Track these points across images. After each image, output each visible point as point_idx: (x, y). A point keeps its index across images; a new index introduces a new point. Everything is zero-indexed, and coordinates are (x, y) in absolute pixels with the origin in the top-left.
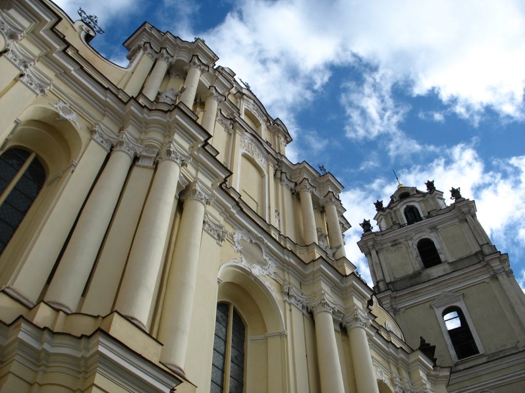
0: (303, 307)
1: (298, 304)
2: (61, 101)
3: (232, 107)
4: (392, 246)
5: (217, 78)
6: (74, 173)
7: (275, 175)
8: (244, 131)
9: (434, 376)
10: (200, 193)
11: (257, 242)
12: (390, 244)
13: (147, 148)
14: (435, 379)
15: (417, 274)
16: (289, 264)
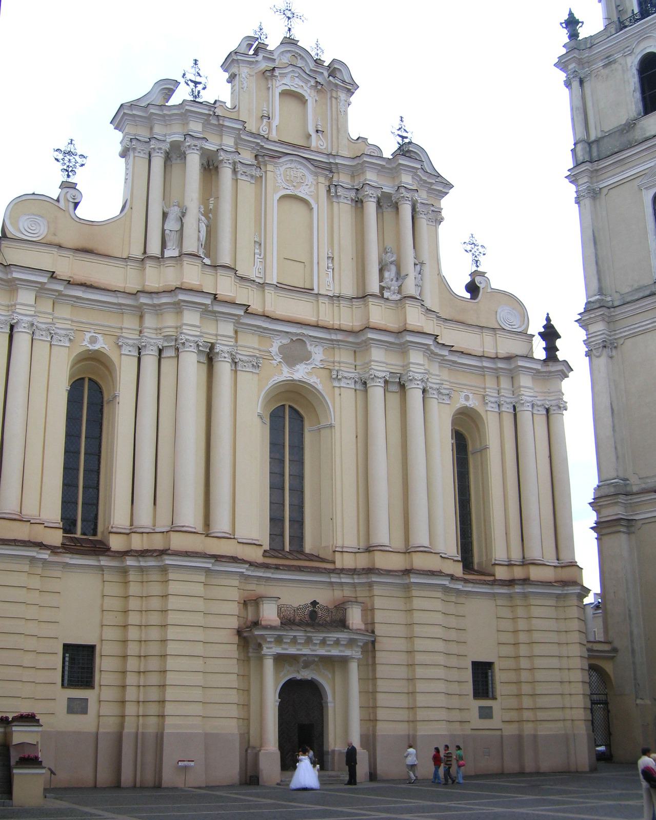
0: (355, 382)
1: (348, 384)
3: (255, 138)
4: (605, 66)
5: (223, 125)
6: (120, 403)
7: (329, 191)
8: (276, 160)
10: (222, 351)
11: (298, 338)
12: (601, 64)
13: (166, 338)
15: (630, 126)
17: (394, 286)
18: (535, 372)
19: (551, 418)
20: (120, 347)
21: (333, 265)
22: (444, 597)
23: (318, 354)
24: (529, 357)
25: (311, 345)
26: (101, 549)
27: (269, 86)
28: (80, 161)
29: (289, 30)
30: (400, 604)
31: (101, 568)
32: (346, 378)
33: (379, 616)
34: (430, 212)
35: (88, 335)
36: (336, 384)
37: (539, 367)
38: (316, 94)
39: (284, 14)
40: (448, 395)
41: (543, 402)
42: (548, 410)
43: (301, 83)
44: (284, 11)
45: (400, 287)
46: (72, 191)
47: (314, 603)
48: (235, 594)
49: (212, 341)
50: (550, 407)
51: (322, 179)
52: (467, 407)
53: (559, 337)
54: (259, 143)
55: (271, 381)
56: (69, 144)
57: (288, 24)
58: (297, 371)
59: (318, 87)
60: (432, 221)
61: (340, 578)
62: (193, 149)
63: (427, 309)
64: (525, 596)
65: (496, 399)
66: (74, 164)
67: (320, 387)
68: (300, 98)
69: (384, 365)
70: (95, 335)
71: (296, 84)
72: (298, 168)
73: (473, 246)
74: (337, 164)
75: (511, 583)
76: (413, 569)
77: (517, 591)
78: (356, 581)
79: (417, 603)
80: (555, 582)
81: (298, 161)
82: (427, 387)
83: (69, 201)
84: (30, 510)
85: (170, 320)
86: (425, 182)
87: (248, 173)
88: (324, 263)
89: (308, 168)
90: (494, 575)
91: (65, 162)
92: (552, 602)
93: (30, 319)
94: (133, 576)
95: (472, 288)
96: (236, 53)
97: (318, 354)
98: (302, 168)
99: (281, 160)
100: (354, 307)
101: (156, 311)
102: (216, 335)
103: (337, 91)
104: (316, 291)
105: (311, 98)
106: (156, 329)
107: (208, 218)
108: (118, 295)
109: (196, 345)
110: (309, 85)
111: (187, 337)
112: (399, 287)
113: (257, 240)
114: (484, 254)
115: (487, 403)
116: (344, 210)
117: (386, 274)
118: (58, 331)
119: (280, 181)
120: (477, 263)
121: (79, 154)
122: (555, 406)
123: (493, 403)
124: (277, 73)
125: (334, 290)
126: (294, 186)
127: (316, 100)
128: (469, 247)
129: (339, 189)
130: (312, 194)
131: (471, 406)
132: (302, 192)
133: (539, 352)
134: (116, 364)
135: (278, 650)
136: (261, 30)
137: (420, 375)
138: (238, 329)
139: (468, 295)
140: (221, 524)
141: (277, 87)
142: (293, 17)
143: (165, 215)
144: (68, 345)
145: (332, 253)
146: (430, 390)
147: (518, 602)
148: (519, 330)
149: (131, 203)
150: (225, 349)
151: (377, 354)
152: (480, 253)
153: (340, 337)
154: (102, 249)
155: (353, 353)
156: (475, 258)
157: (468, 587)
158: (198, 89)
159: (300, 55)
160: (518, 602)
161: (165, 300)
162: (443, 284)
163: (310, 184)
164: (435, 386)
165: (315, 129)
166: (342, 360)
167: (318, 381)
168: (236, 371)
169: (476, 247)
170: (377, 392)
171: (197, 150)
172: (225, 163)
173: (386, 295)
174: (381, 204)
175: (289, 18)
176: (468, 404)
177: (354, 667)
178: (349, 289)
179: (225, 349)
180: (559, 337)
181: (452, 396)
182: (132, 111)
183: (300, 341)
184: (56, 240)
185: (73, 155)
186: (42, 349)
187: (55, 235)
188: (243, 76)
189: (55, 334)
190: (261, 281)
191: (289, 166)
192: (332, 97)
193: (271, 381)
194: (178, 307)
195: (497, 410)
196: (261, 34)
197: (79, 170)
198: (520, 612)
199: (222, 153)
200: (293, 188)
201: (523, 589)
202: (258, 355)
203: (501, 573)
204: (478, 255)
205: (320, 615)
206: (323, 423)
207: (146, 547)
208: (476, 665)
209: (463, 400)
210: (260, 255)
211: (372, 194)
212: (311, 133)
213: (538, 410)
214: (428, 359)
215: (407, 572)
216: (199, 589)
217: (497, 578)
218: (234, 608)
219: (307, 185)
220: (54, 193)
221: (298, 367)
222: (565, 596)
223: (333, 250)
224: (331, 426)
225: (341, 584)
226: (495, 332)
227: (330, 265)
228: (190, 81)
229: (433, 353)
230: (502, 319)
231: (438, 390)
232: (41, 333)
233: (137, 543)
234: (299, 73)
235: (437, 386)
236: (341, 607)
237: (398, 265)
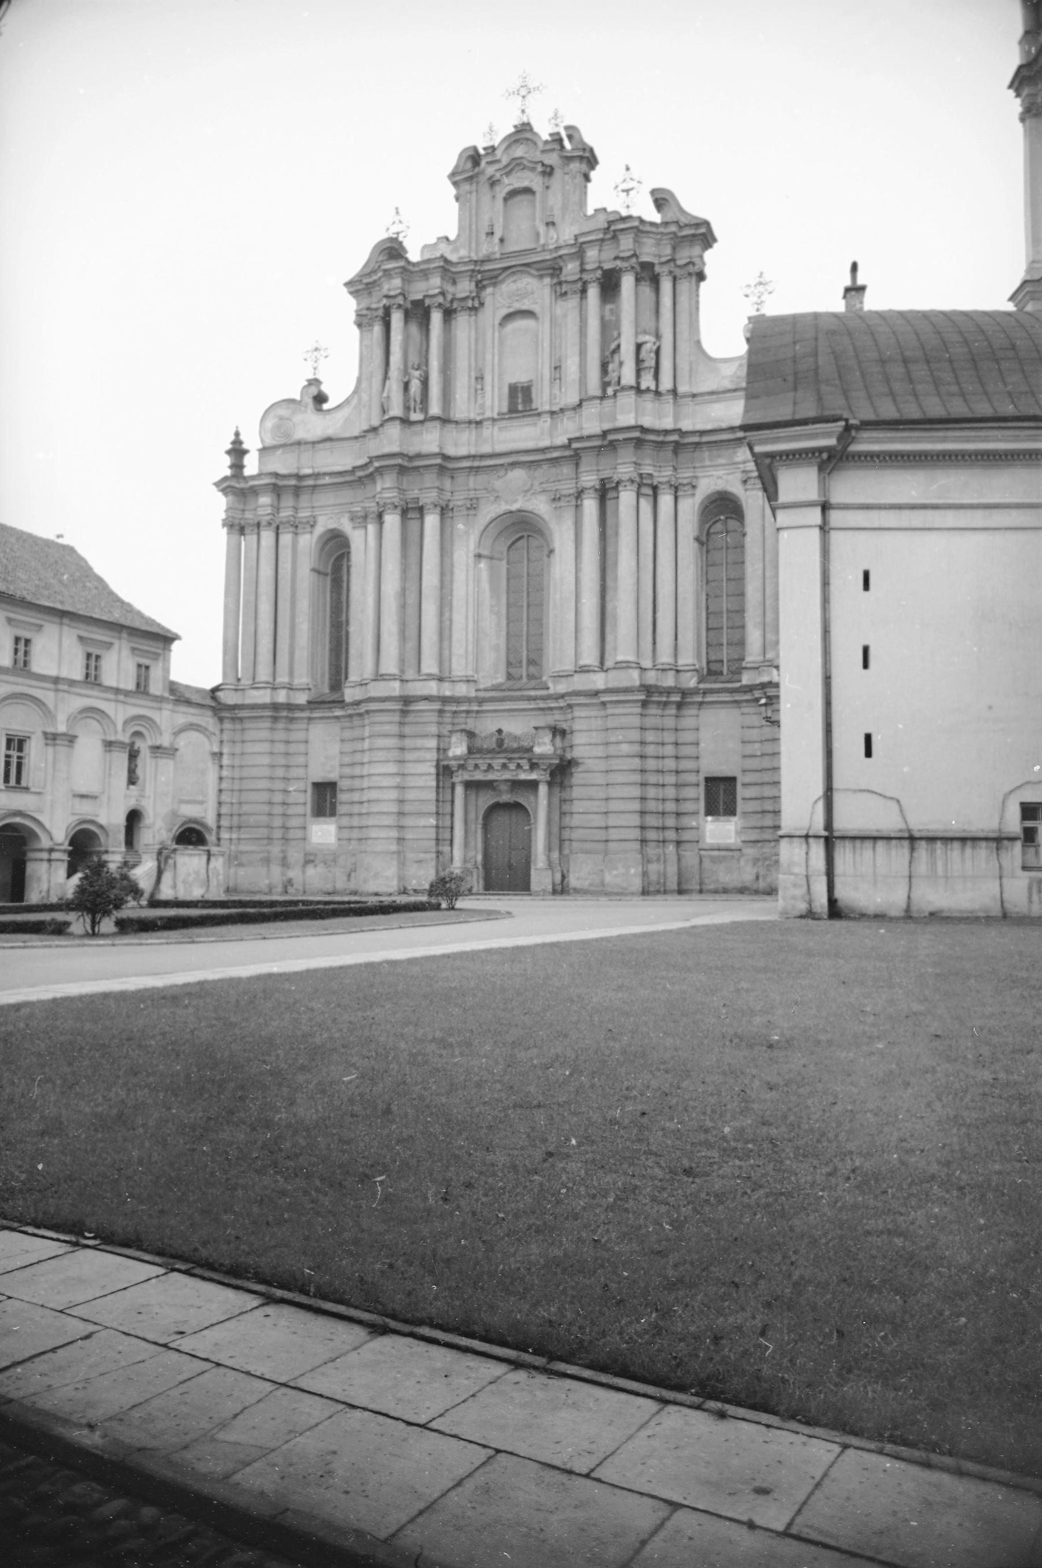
47: (500, 731)
74: (560, 257)
99: (501, 278)
132: (525, 305)
135: (467, 776)
150: (428, 501)
164: (665, 480)
177: (543, 789)
190: (478, 419)
191: (512, 279)
208: (711, 782)
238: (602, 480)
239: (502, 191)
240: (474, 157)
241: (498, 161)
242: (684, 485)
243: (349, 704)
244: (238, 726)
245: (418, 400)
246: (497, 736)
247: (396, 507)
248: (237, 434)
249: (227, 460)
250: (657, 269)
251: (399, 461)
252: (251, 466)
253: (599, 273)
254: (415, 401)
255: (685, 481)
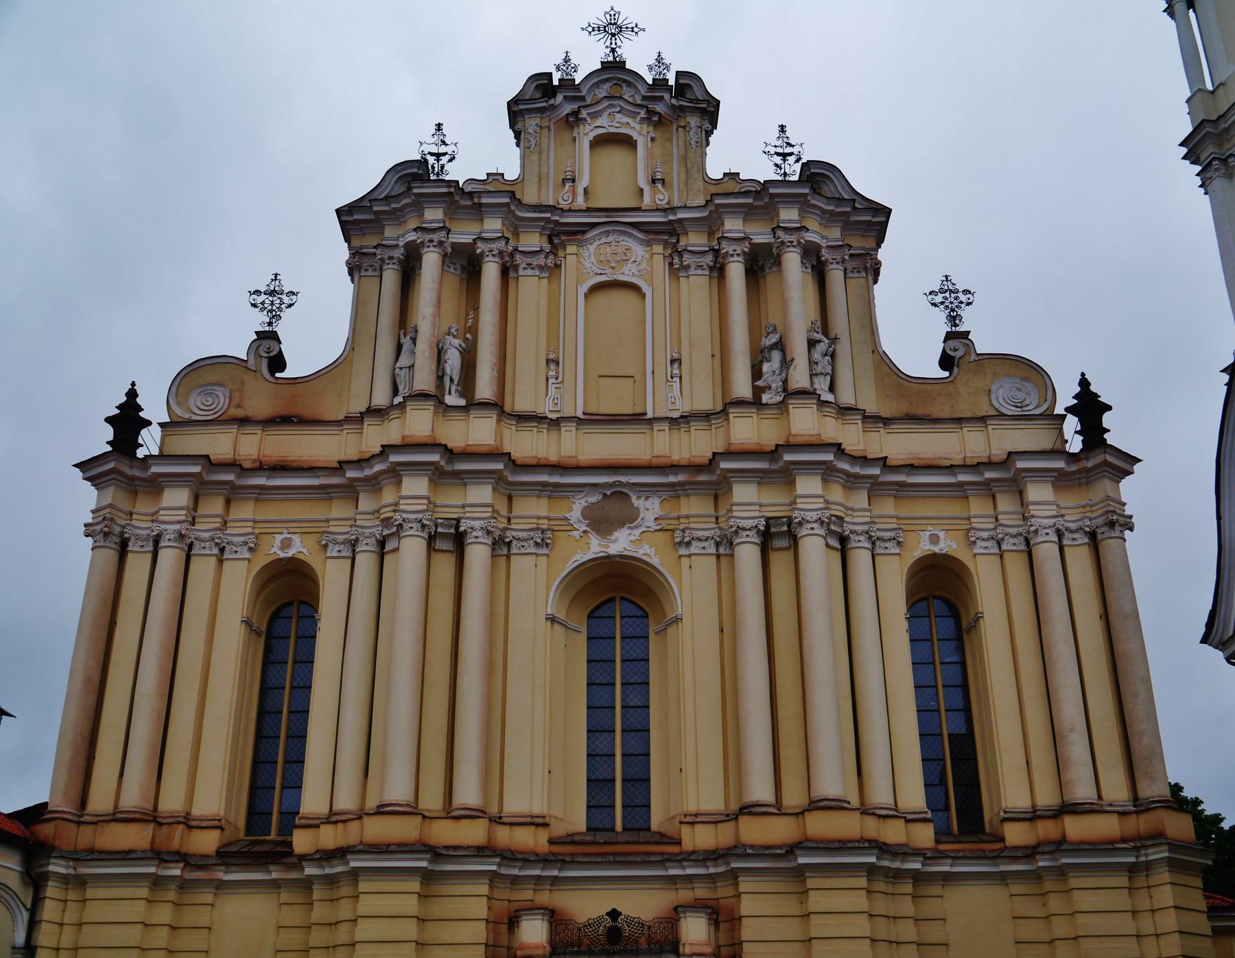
0: (718, 544)
1: (704, 548)
2: (275, 535)
3: (541, 212)
5: (480, 205)
7: (671, 264)
9: (1079, 471)
10: (472, 528)
11: (615, 489)
13: (384, 524)
14: (1084, 475)
16: (681, 484)
17: (777, 384)
18: (1056, 474)
19: (1101, 546)
20: (326, 546)
21: (680, 372)
22: (889, 889)
23: (650, 509)
24: (1058, 451)
25: (639, 498)
26: (282, 854)
27: (574, 135)
28: (286, 300)
29: (613, 50)
30: (789, 905)
31: (275, 885)
32: (699, 539)
33: (748, 930)
34: (847, 257)
35: (279, 538)
36: (683, 551)
37: (1060, 464)
38: (651, 129)
39: (605, 31)
40: (894, 539)
41: (1080, 523)
42: (1093, 536)
43: (625, 120)
44: (605, 27)
45: (785, 382)
46: (273, 343)
47: (614, 914)
48: (480, 908)
49: (455, 516)
50: (1097, 530)
51: (658, 248)
52: (935, 554)
53: (1109, 408)
54: (550, 218)
55: (570, 563)
56: (272, 280)
57: (611, 44)
58: (616, 541)
59: (656, 121)
60: (859, 272)
61: (684, 868)
62: (428, 247)
63: (841, 408)
64: (1062, 872)
65: (992, 533)
66: (278, 306)
67: (655, 561)
68: (627, 142)
69: (757, 508)
70: (289, 536)
71: (618, 122)
72: (619, 240)
73: (947, 295)
74: (680, 221)
75: (1029, 852)
76: (807, 840)
77: (1041, 864)
78: (712, 870)
79: (816, 901)
80: (1124, 840)
81: (619, 230)
82: (844, 532)
83: (261, 357)
84: (172, 801)
85: (388, 496)
86: (832, 213)
87: (535, 263)
88: (663, 369)
89: (635, 237)
90: (1003, 840)
91: (266, 306)
92: (1123, 881)
93: (177, 527)
94: (316, 895)
95: (946, 361)
96: (516, 101)
97: (650, 509)
98: (626, 239)
100: (713, 427)
101: (374, 486)
102: (463, 506)
103: (685, 117)
104: (650, 415)
105: (642, 136)
106: (373, 513)
107: (466, 340)
108: (319, 474)
109: (420, 525)
110: (638, 119)
111: (405, 516)
112: (783, 382)
113: (552, 356)
114: (969, 304)
115: (974, 543)
116: (697, 286)
117: (766, 367)
118: (235, 539)
119: (588, 265)
120: (955, 320)
121: (286, 291)
122: (1104, 526)
123: (987, 540)
124: (584, 114)
125: (682, 406)
126: (613, 268)
127: (653, 139)
128: (939, 298)
129: (686, 256)
130: (641, 274)
131: (944, 552)
132: (626, 274)
133: (1075, 444)
134: (318, 573)
136: (566, 62)
137: (815, 513)
138: (512, 492)
139: (946, 374)
140: (468, 793)
141: (586, 134)
142: (621, 31)
143: (399, 348)
144: (247, 555)
145: (679, 353)
146: (851, 535)
147: (1049, 885)
148: (1037, 412)
149: (353, 342)
150: (477, 524)
151: (743, 492)
152: (961, 302)
153: (681, 478)
154: (308, 412)
155: (712, 499)
156: (952, 313)
157: (945, 865)
158: (441, 162)
159: (625, 81)
160: (1049, 885)
161: (378, 467)
162: (884, 366)
163: (639, 259)
164: (860, 528)
165: (650, 181)
166: (693, 512)
167: (652, 552)
168: (508, 557)
169: (953, 295)
170: (748, 554)
171: (434, 246)
172: (487, 256)
173: (765, 398)
174: (760, 263)
175: (613, 35)
176: (942, 547)
178: (706, 401)
179: (477, 524)
180: (1109, 408)
181: (901, 540)
182: (352, 216)
183: (619, 494)
184: (240, 413)
185: (278, 294)
186: (203, 568)
187: (239, 406)
188: (531, 130)
189: (247, 543)
190: (554, 416)
191: (604, 240)
192: (678, 127)
193: (570, 563)
194: (396, 474)
195: (996, 550)
196: (567, 68)
197: (286, 314)
198: (1056, 903)
199: (479, 244)
200: (610, 270)
201: (1056, 860)
202: (545, 527)
203: (1016, 834)
204: (957, 307)
205: (627, 934)
206: (670, 615)
207: (341, 842)
209: (927, 543)
210: (557, 379)
211: (735, 251)
212: (642, 187)
213: (1074, 539)
214: (844, 487)
215: (792, 849)
216: (411, 905)
217: (1008, 844)
218: (478, 932)
219: (635, 261)
220: (239, 348)
221: (616, 534)
222: (1148, 867)
223: (680, 348)
224: (677, 620)
225: (689, 879)
226: (985, 422)
227: (676, 371)
228: (428, 155)
229: (848, 475)
230: (1001, 400)
231: (867, 533)
232: (203, 545)
233: (329, 837)
234: (621, 106)
235: (866, 528)
236: (673, 918)
237: (781, 346)
238: (768, 520)
239: (587, 133)
240: (541, 85)
241: (583, 98)
242: (884, 540)
243: (303, 858)
244: (72, 895)
245: (456, 378)
246: (608, 922)
247: (424, 526)
248: (132, 394)
249: (109, 433)
250: (826, 255)
251: (435, 457)
252: (150, 441)
253: (746, 247)
254: (452, 380)
255: (886, 535)
